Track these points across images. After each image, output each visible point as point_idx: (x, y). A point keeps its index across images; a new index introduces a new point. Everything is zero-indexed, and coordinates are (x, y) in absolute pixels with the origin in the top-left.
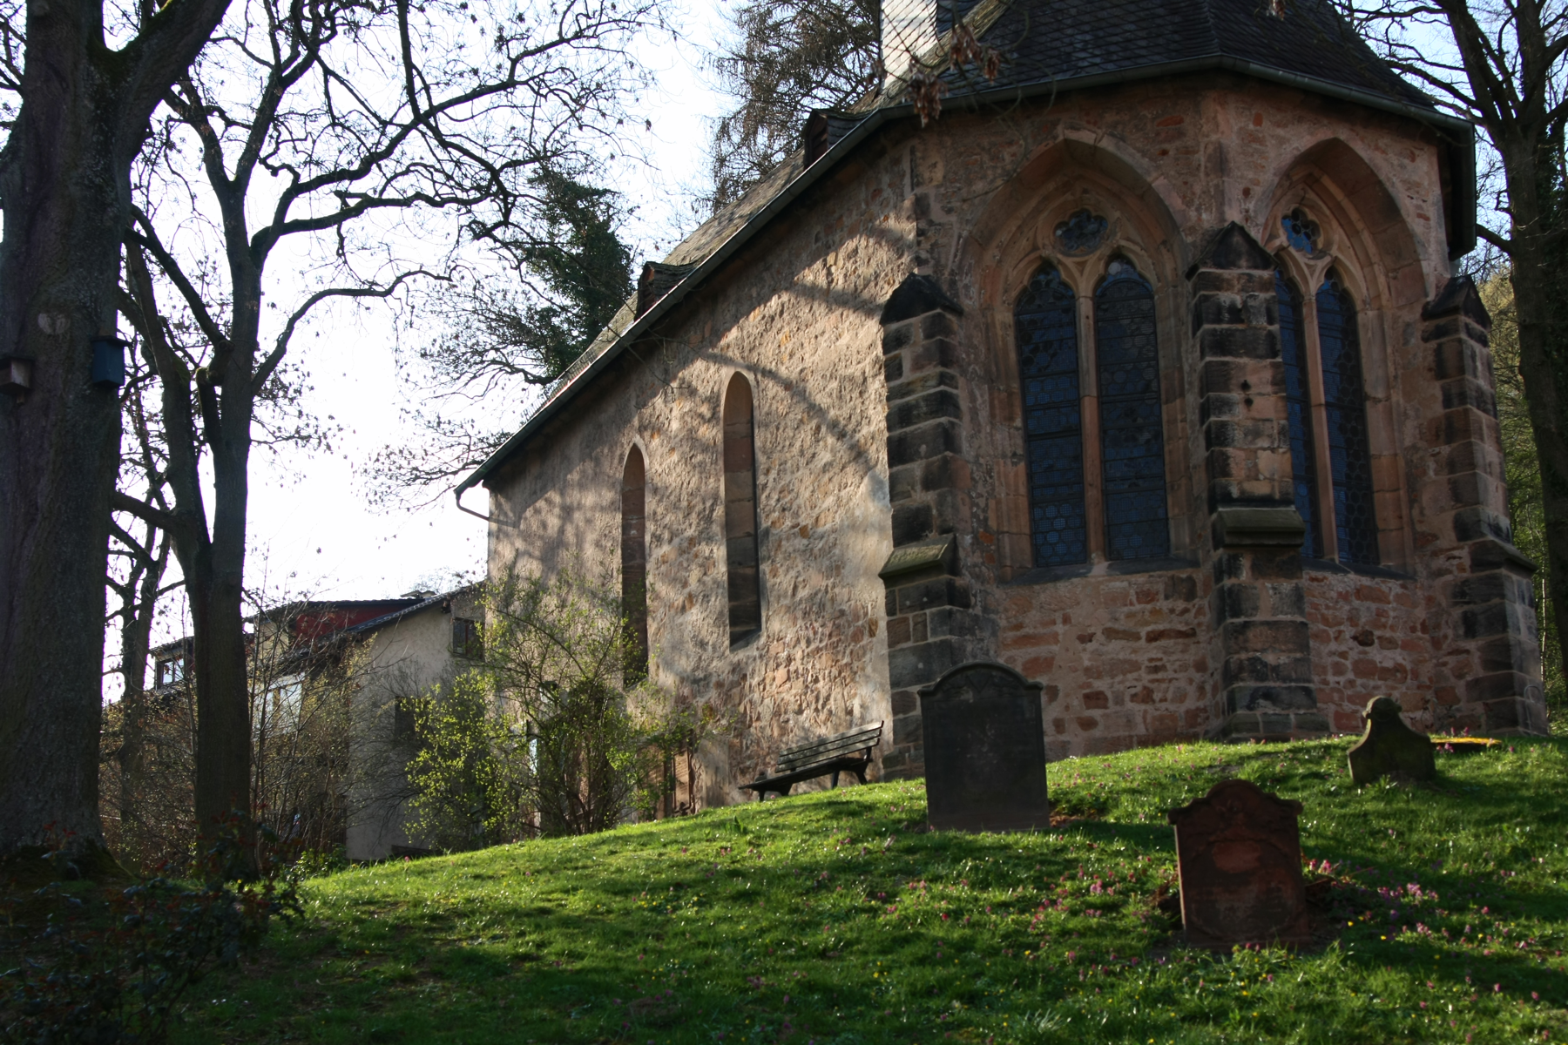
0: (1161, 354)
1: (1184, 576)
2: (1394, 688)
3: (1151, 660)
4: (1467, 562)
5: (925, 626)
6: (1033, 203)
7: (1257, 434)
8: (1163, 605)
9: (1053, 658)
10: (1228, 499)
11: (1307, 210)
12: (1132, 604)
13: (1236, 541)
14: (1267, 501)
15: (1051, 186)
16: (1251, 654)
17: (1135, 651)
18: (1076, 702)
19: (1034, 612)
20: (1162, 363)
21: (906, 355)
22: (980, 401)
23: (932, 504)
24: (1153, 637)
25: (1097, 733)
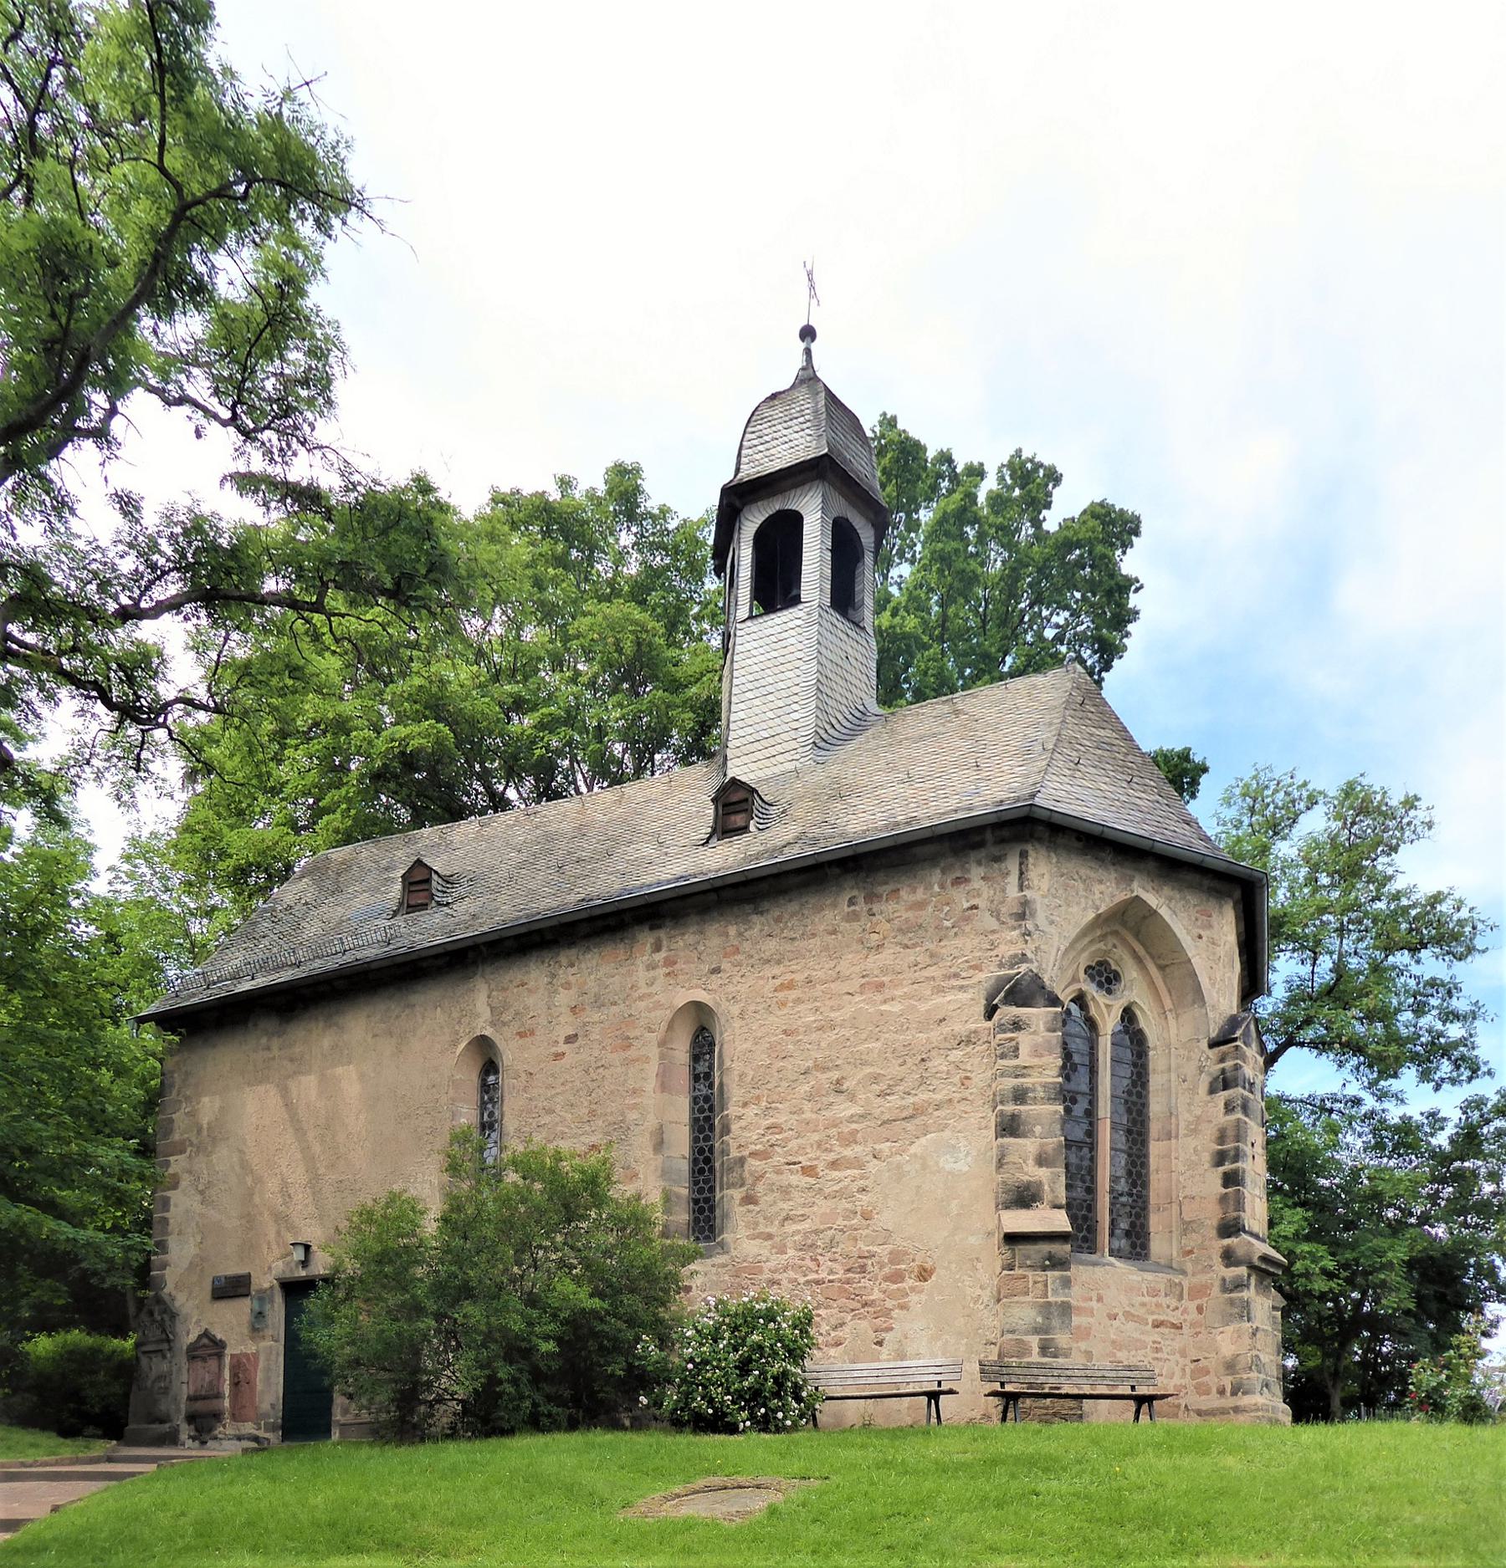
3: (1154, 1342)
5: (1046, 1286)
23: (1045, 1181)
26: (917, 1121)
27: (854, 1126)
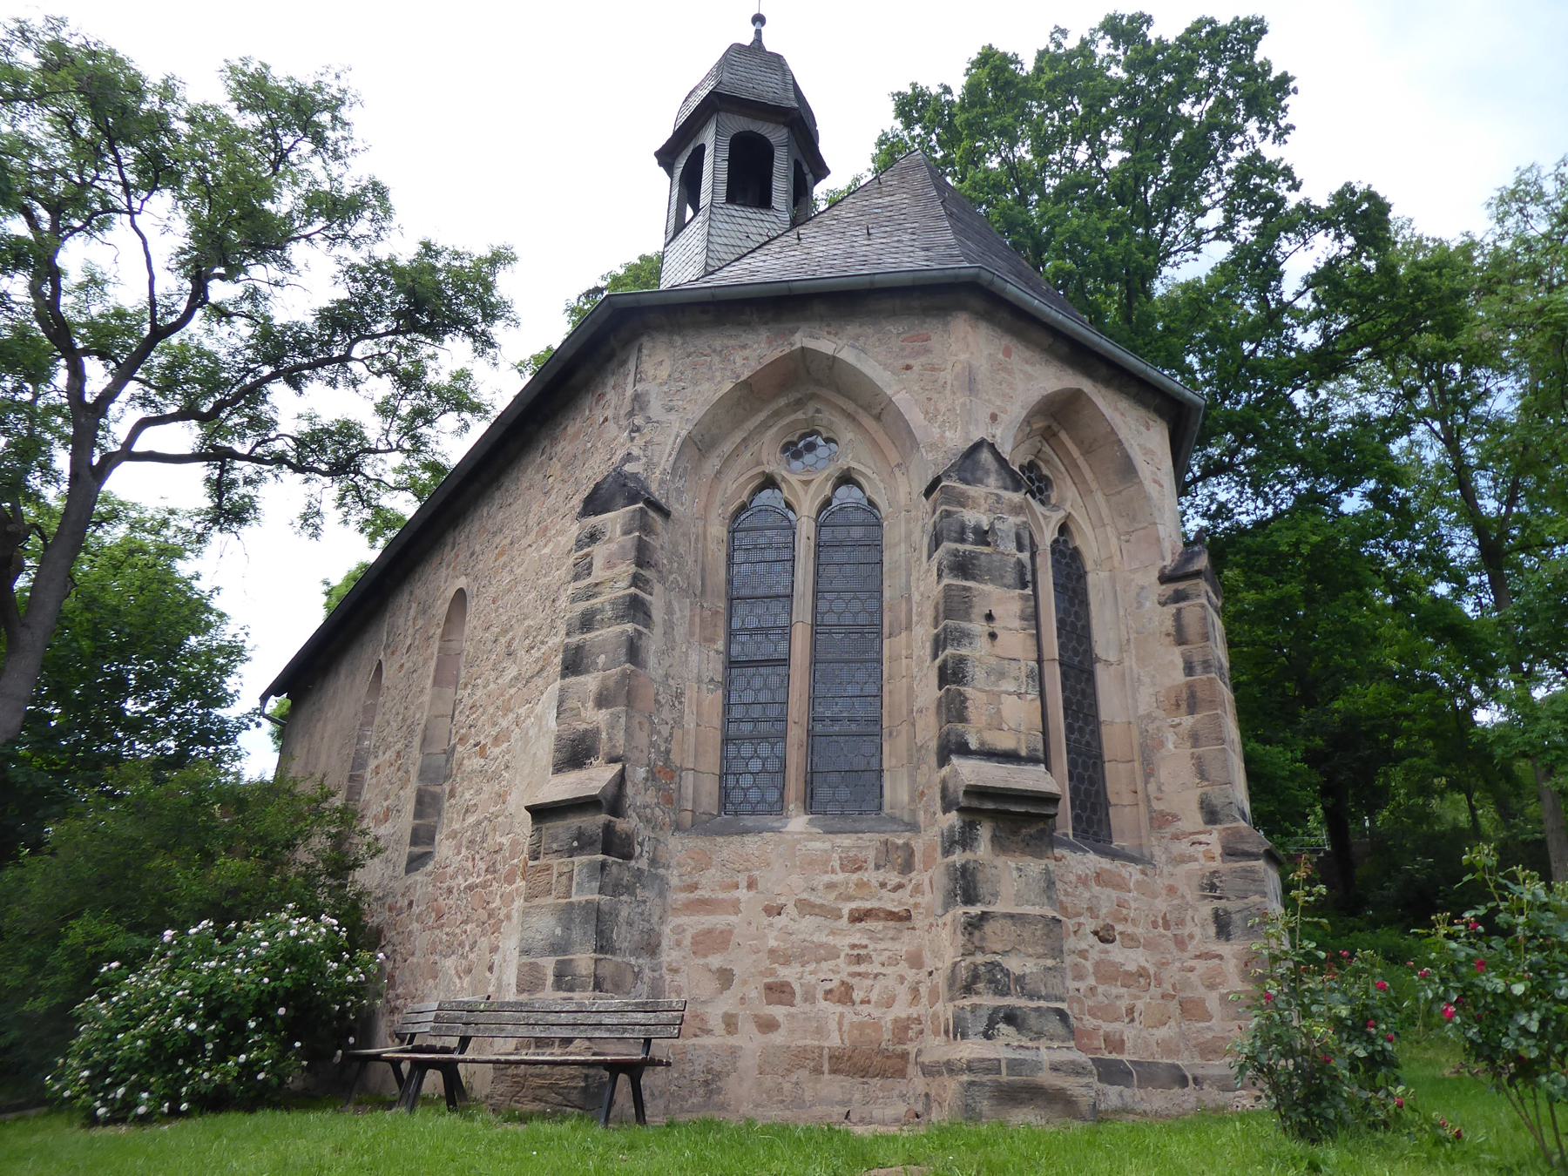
0: (886, 584)
1: (900, 842)
2: (1139, 998)
3: (853, 946)
4: (1217, 850)
5: (571, 879)
6: (762, 416)
7: (1002, 675)
8: (872, 876)
9: (731, 932)
10: (964, 750)
11: (1041, 464)
12: (833, 871)
13: (975, 804)
14: (1010, 757)
15: (782, 402)
16: (989, 958)
17: (832, 933)
18: (754, 992)
19: (713, 871)
20: (887, 594)
21: (599, 552)
22: (678, 614)
23: (603, 726)
24: (858, 917)
25: (778, 1038)
26: (545, 674)
27: (513, 691)
